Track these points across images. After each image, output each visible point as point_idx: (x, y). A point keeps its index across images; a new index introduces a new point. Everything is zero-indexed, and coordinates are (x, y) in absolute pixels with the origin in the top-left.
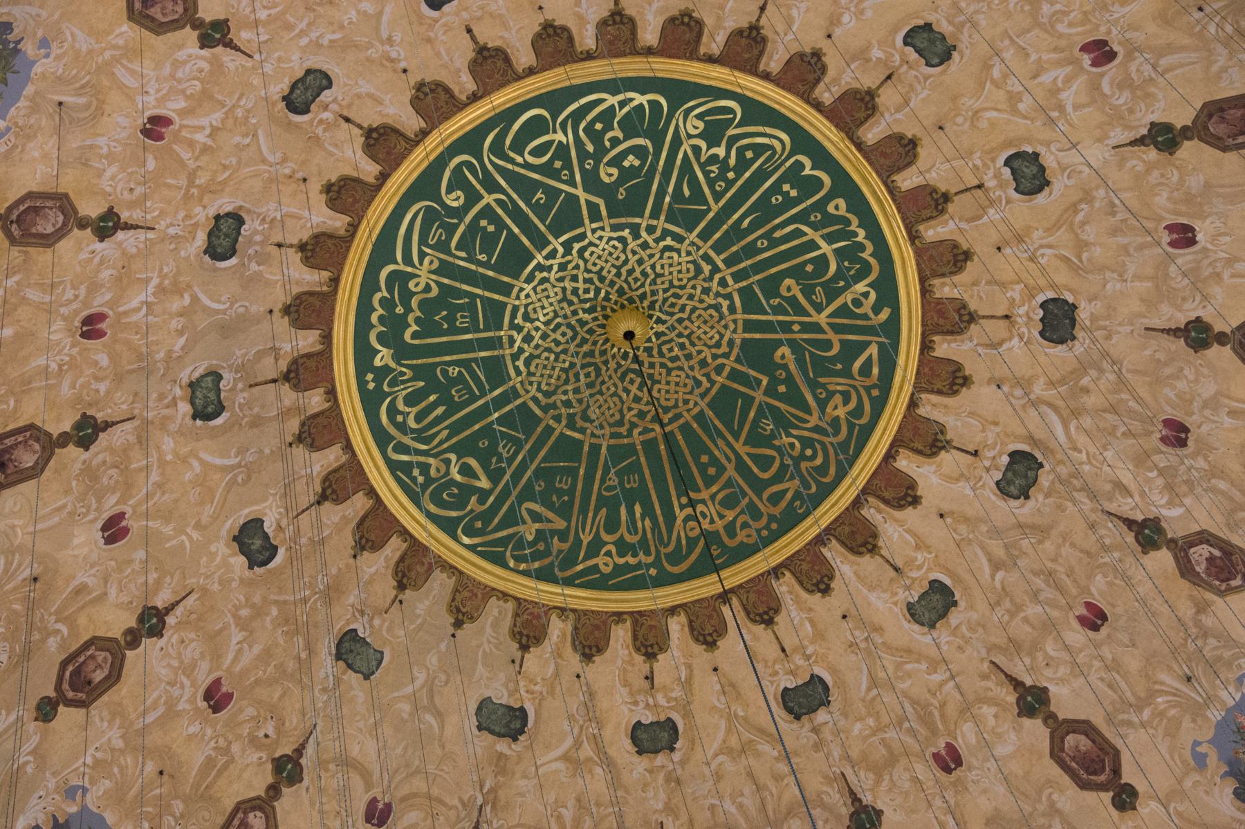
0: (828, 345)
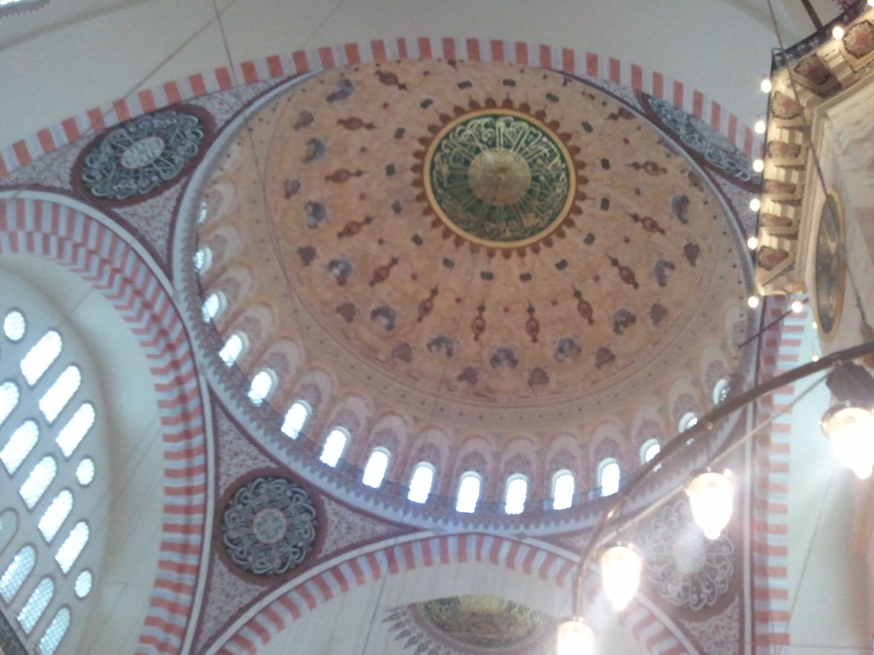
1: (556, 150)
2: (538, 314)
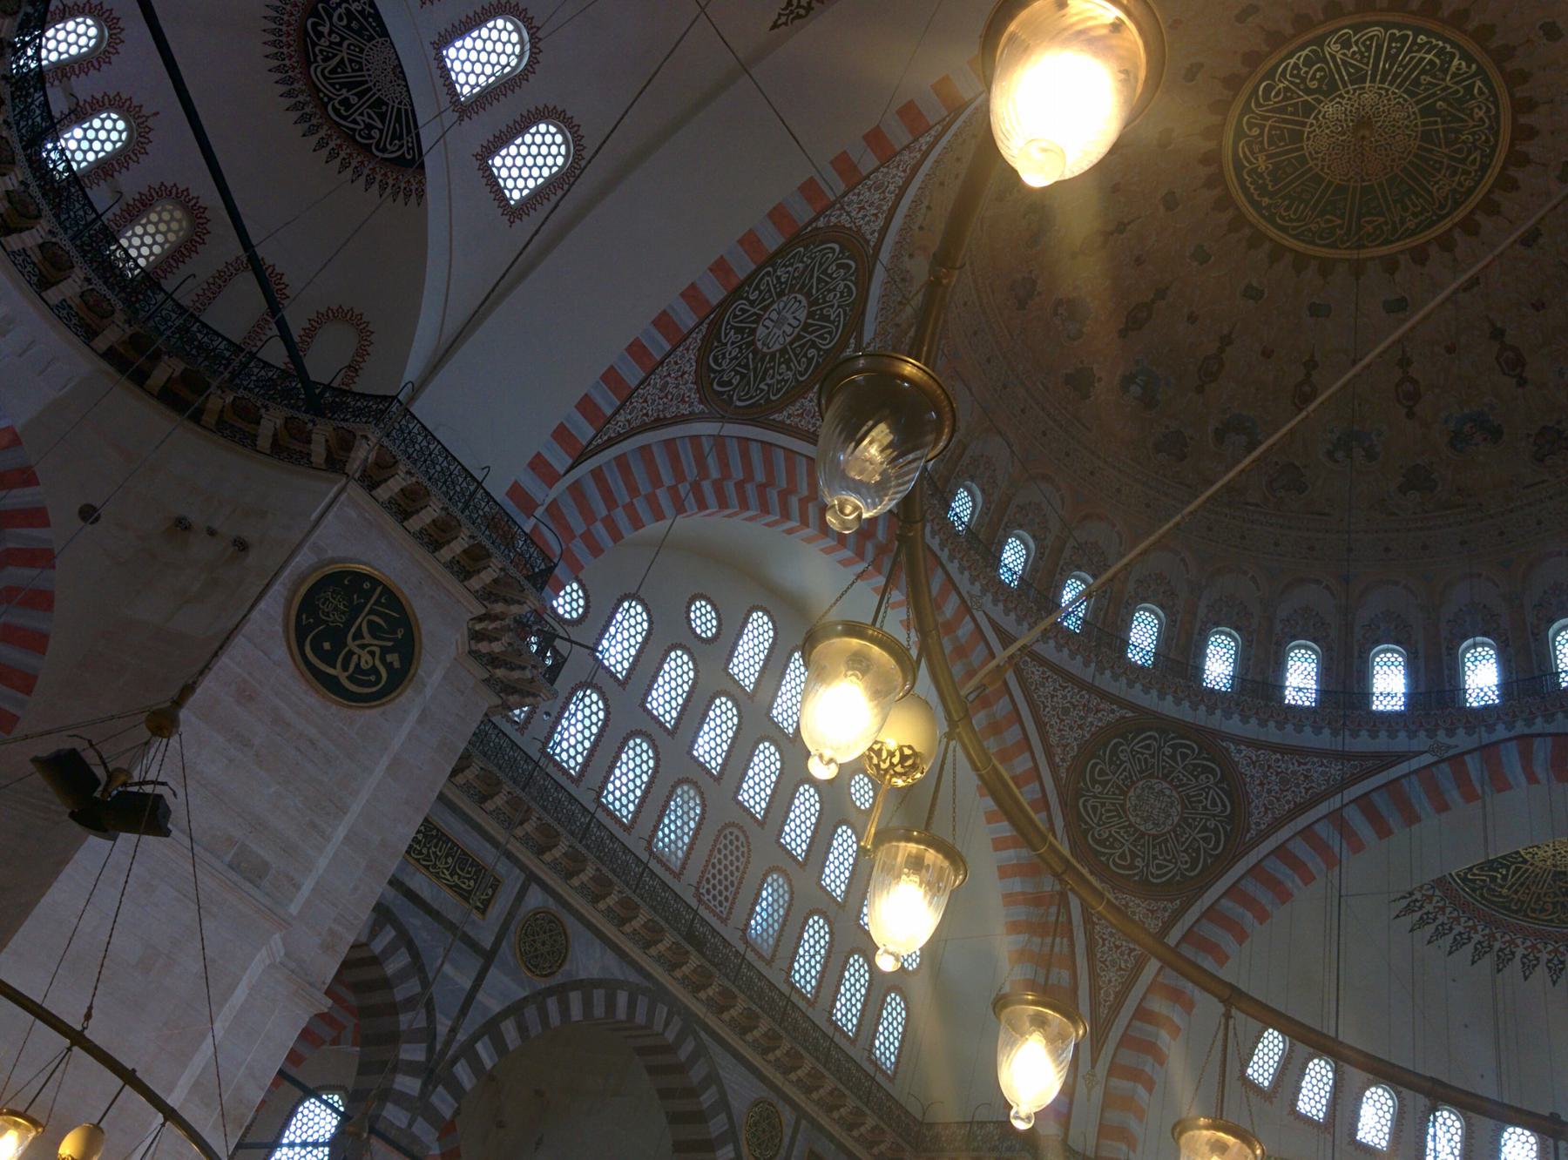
1: (1449, 48)
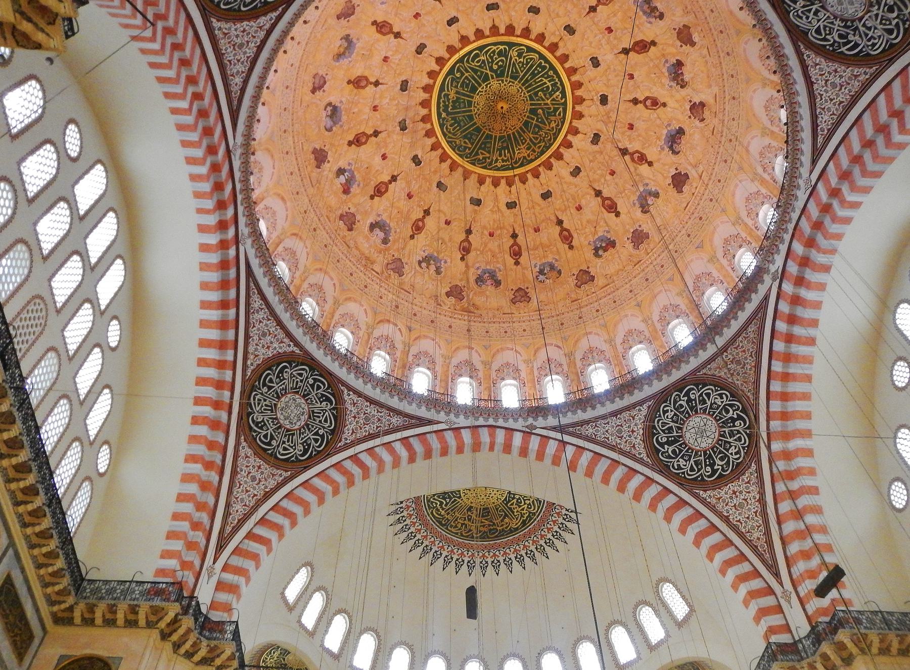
0: (550, 108)
2: (520, 239)
